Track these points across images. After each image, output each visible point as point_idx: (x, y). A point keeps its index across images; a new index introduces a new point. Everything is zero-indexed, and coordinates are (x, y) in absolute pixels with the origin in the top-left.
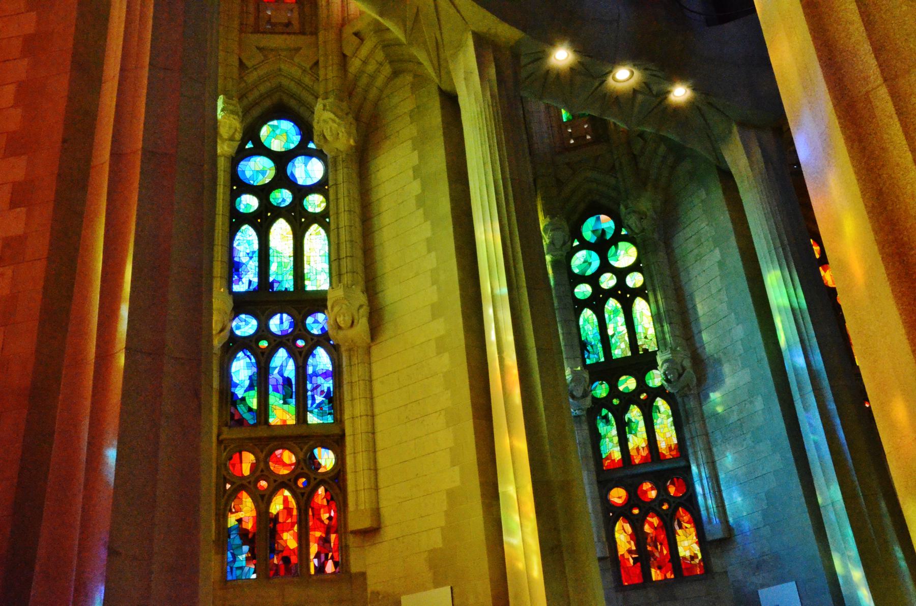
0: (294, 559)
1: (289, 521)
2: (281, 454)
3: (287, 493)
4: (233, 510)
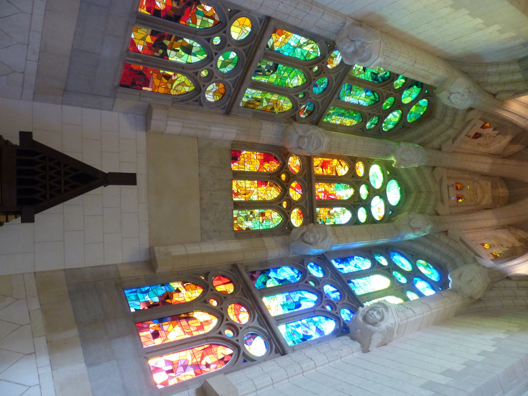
4: (185, 285)
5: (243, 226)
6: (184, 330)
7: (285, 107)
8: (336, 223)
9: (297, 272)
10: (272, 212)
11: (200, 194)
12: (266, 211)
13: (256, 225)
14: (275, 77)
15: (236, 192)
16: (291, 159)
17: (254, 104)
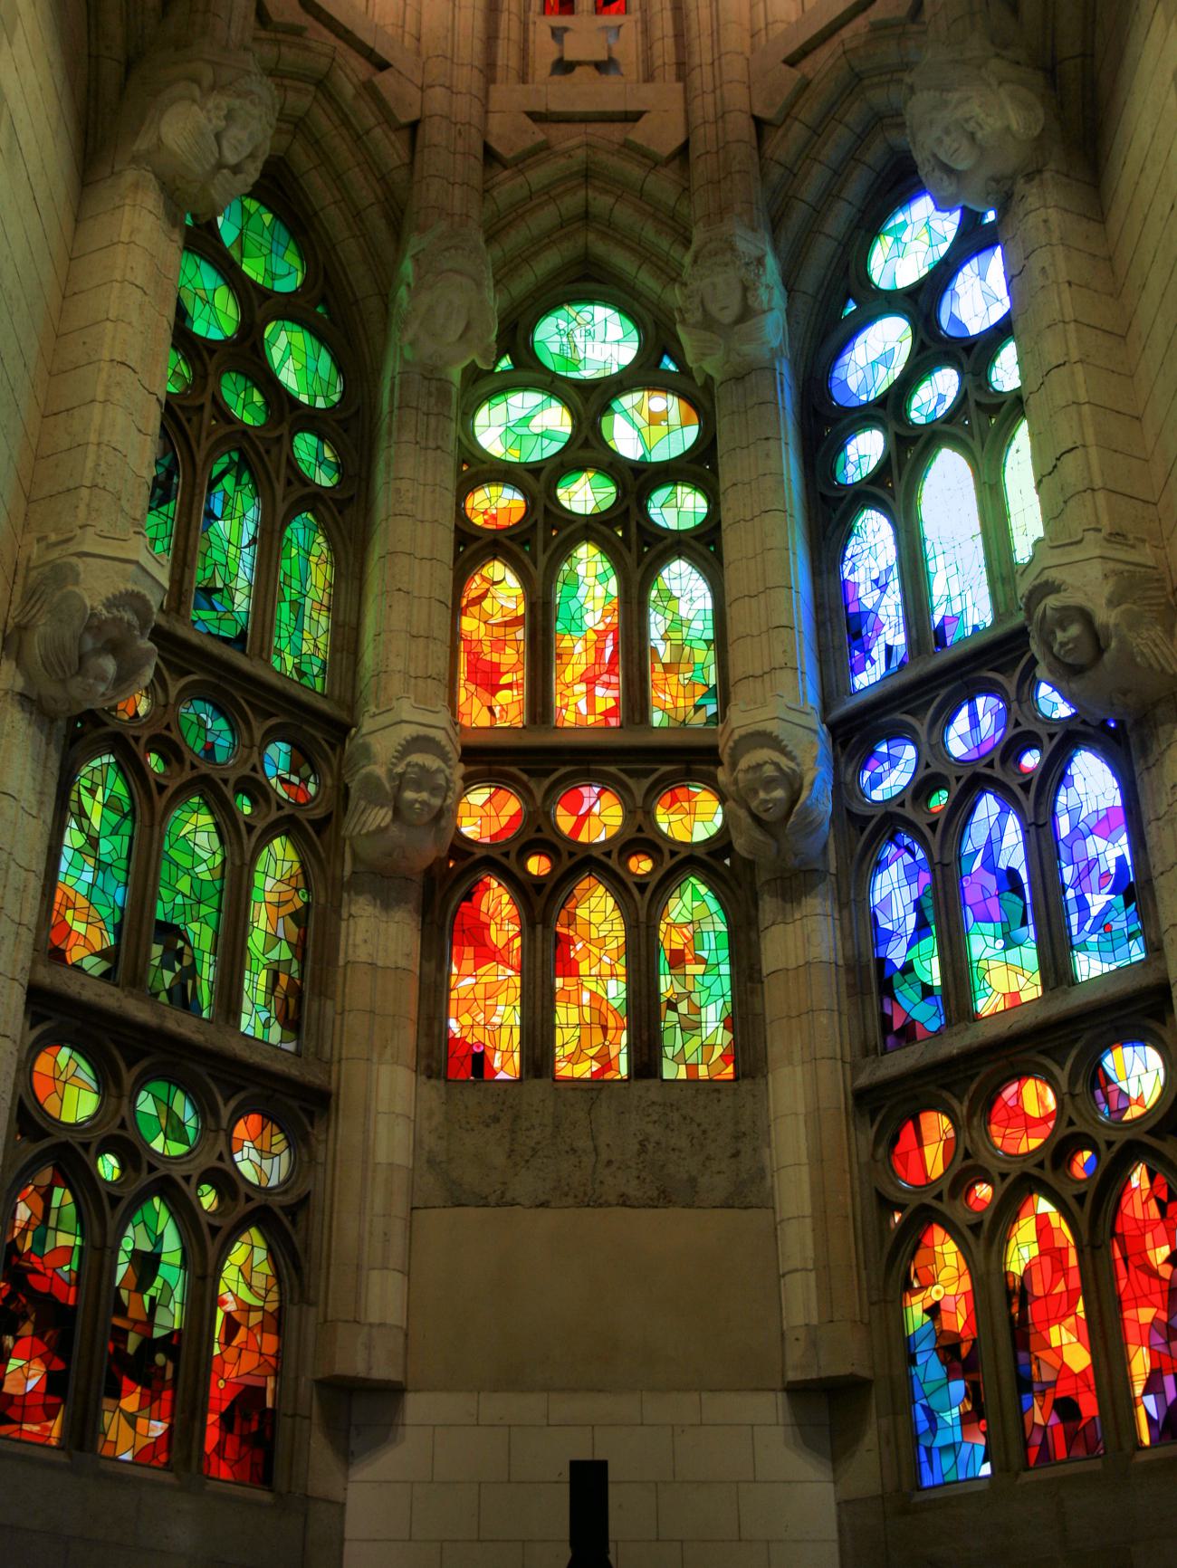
0: (1088, 1406)
1: (1061, 1287)
2: (1019, 1094)
3: (1044, 1206)
4: (916, 1285)
5: (719, 1042)
6: (1061, 1314)
7: (287, 865)
8: (710, 635)
9: (891, 850)
10: (668, 920)
11: (610, 1205)
12: (666, 945)
13: (716, 990)
14: (195, 927)
15: (596, 1066)
16: (470, 829)
17: (286, 997)
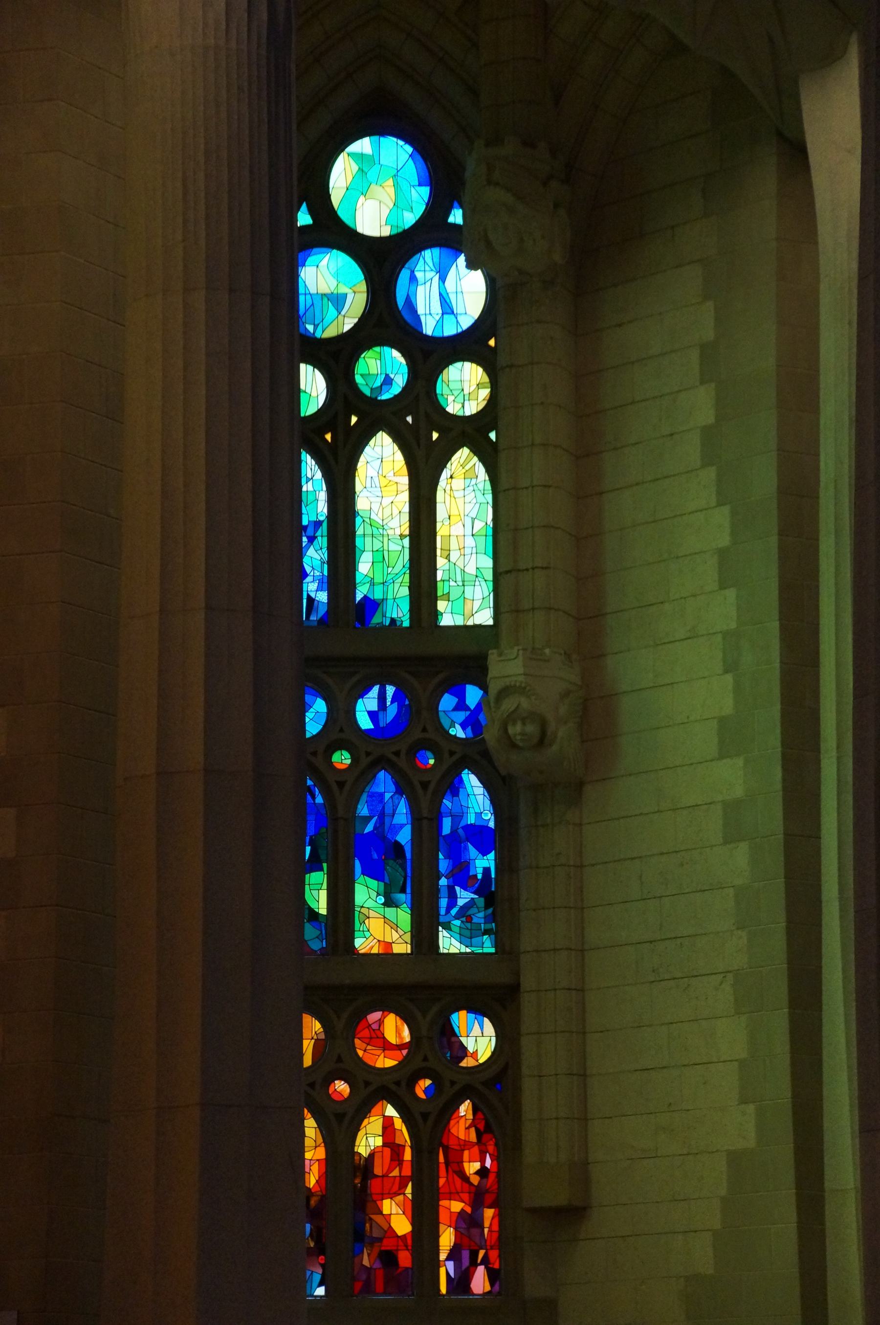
0: (405, 1259)
1: (396, 1173)
2: (381, 1022)
3: (390, 1111)
